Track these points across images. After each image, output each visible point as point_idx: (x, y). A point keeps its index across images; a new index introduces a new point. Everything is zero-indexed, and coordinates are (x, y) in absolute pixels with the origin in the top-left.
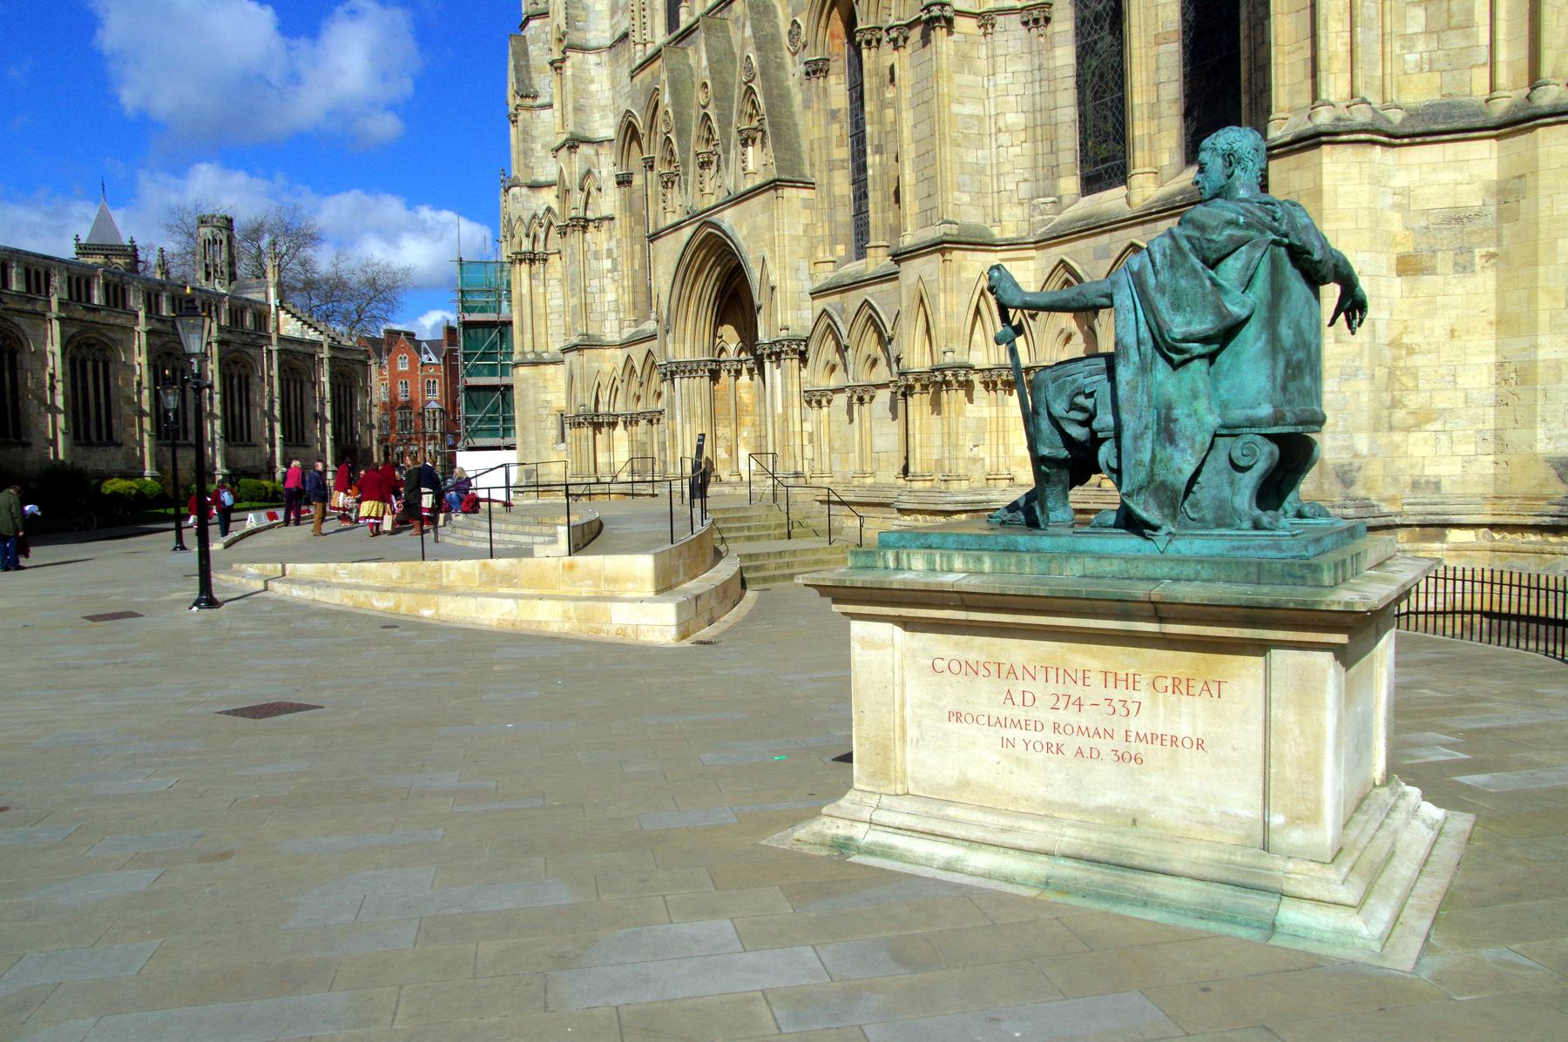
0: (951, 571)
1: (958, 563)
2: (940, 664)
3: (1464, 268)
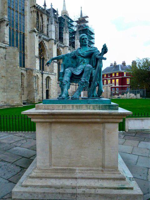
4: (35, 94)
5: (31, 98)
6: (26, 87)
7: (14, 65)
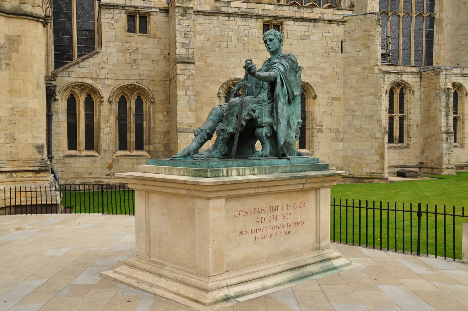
0: (245, 175)
1: (247, 172)
2: (237, 213)
4: (445, 145)
5: (430, 158)
6: (417, 126)
7: (365, 65)
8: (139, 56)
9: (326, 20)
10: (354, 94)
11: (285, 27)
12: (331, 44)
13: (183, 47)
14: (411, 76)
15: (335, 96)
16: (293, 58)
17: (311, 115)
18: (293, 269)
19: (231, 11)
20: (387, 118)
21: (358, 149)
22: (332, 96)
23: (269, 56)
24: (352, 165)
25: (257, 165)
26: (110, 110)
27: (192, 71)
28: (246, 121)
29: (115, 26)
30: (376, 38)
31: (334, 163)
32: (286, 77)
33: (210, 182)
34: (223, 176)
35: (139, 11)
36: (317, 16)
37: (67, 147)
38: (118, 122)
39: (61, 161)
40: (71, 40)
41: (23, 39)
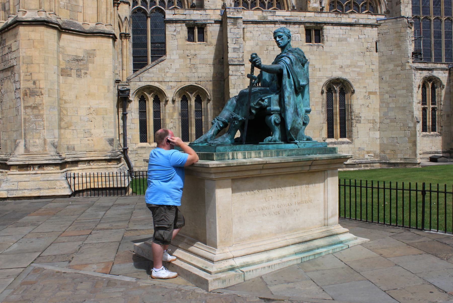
0: (251, 158)
1: (253, 155)
3: (79, 76)
8: (198, 62)
9: (361, 24)
10: (388, 88)
11: (325, 31)
12: (366, 45)
13: (234, 52)
14: (441, 72)
15: (371, 91)
16: (300, 52)
17: (351, 107)
18: (299, 243)
19: (276, 19)
20: (421, 109)
21: (393, 138)
22: (368, 90)
23: (278, 51)
24: (388, 152)
25: (264, 149)
26: (174, 108)
27: (242, 72)
28: (256, 109)
29: (177, 37)
30: (406, 39)
31: (372, 150)
32: (292, 69)
33: (213, 164)
34: (229, 159)
35: (197, 23)
36: (353, 21)
37: (139, 140)
38: (180, 117)
39: (134, 152)
40: (146, 52)
41: (97, 52)
